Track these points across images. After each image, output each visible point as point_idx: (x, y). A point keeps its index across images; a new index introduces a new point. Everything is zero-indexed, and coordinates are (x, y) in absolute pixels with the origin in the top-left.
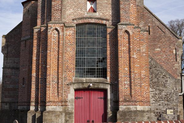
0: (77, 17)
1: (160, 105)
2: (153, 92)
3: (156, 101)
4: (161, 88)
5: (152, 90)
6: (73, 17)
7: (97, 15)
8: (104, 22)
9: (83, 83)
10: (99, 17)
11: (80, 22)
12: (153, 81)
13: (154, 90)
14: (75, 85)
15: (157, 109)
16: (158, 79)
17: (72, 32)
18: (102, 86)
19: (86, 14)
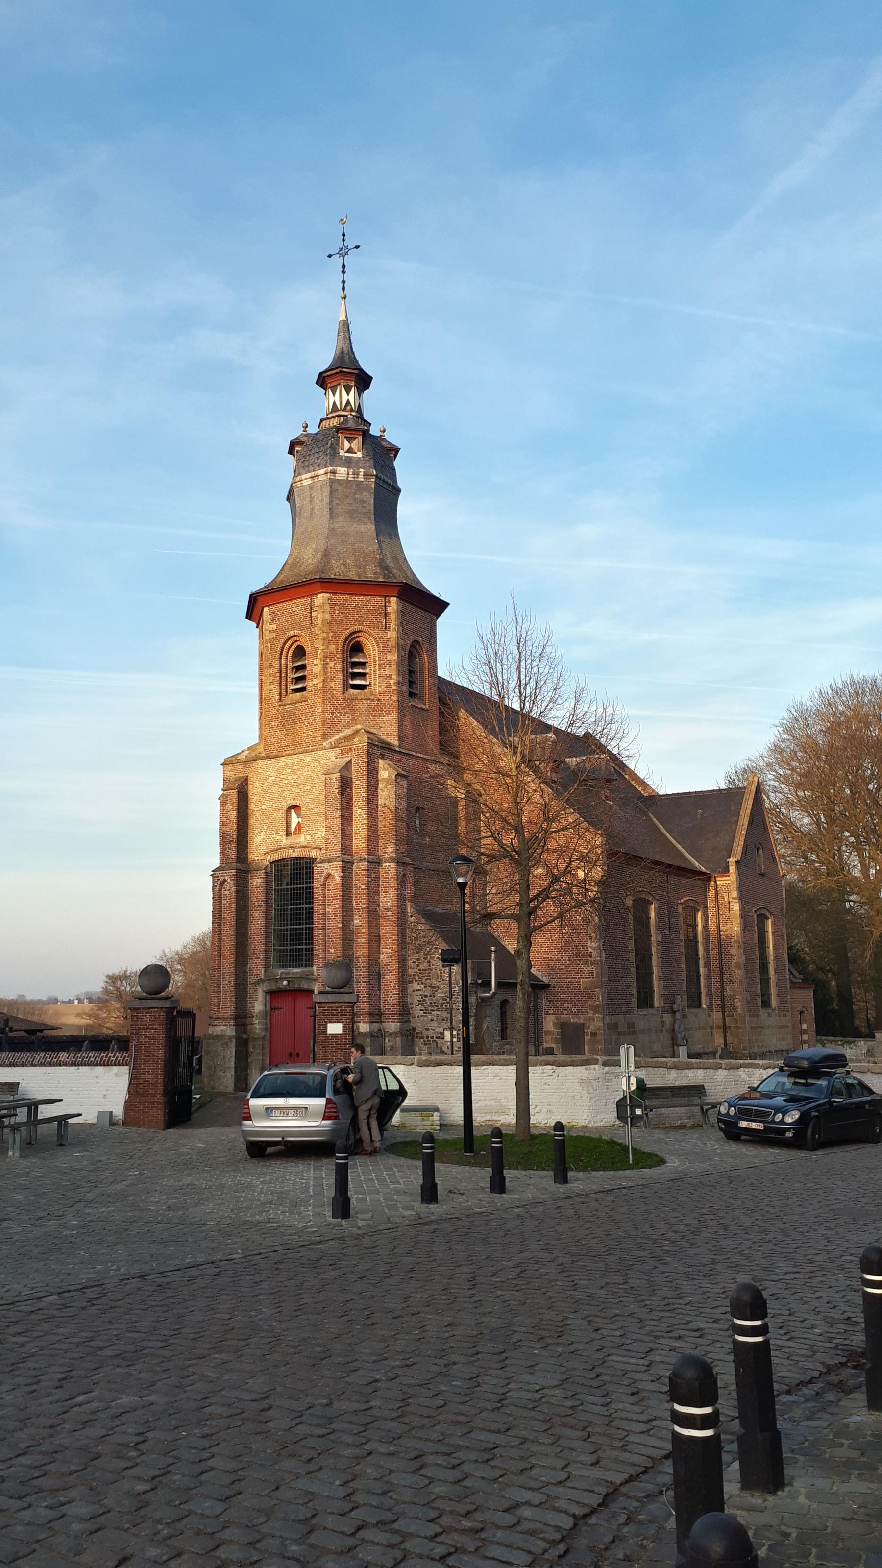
0: (272, 848)
1: (432, 1020)
2: (420, 993)
3: (426, 1011)
4: (434, 982)
5: (419, 988)
6: (264, 848)
7: (302, 839)
8: (313, 854)
9: (276, 980)
10: (305, 844)
11: (277, 857)
12: (421, 967)
13: (422, 986)
14: (266, 983)
15: (427, 1029)
16: (429, 962)
17: (260, 880)
18: (305, 985)
19: (284, 841)
